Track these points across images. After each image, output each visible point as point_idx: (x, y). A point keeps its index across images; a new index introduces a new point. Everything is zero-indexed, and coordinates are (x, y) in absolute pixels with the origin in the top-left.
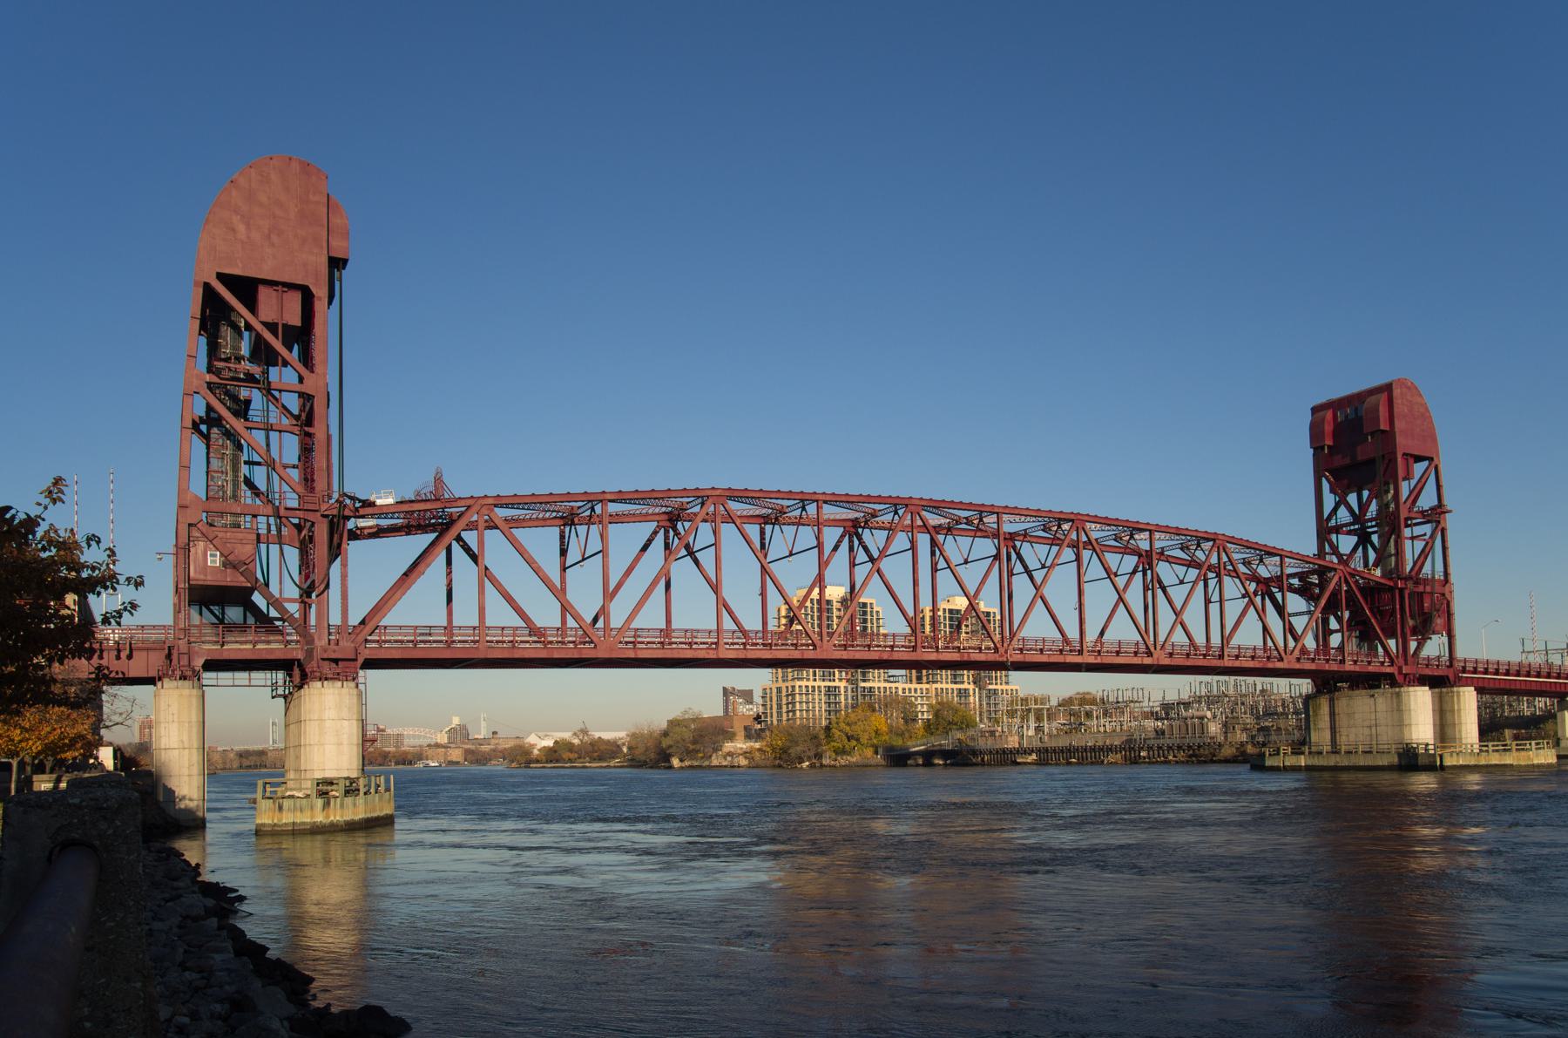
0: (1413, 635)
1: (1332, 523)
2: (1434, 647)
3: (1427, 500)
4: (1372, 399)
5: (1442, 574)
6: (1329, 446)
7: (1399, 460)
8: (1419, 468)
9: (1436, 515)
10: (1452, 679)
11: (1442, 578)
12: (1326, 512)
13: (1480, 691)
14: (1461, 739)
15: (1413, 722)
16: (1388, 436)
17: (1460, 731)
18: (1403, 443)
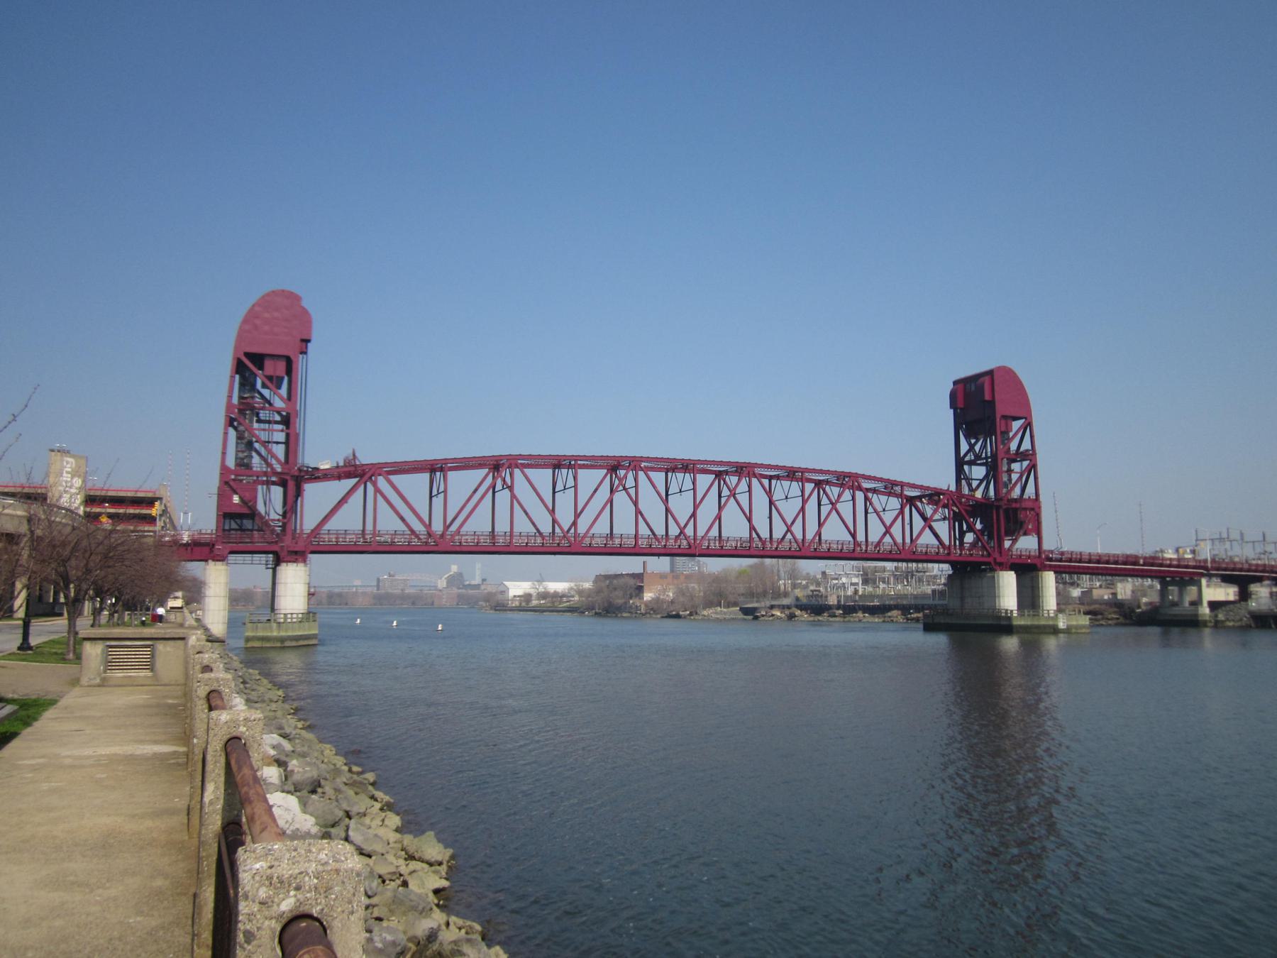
0: (1007, 535)
1: (967, 459)
2: (1026, 544)
3: (1026, 445)
4: (982, 379)
5: (1034, 495)
6: (961, 409)
7: (998, 420)
8: (1016, 425)
9: (1030, 456)
10: (1039, 565)
11: (1034, 497)
12: (962, 453)
13: (1055, 572)
14: (1043, 607)
15: (1001, 594)
16: (992, 403)
17: (1043, 602)
18: (1001, 410)
